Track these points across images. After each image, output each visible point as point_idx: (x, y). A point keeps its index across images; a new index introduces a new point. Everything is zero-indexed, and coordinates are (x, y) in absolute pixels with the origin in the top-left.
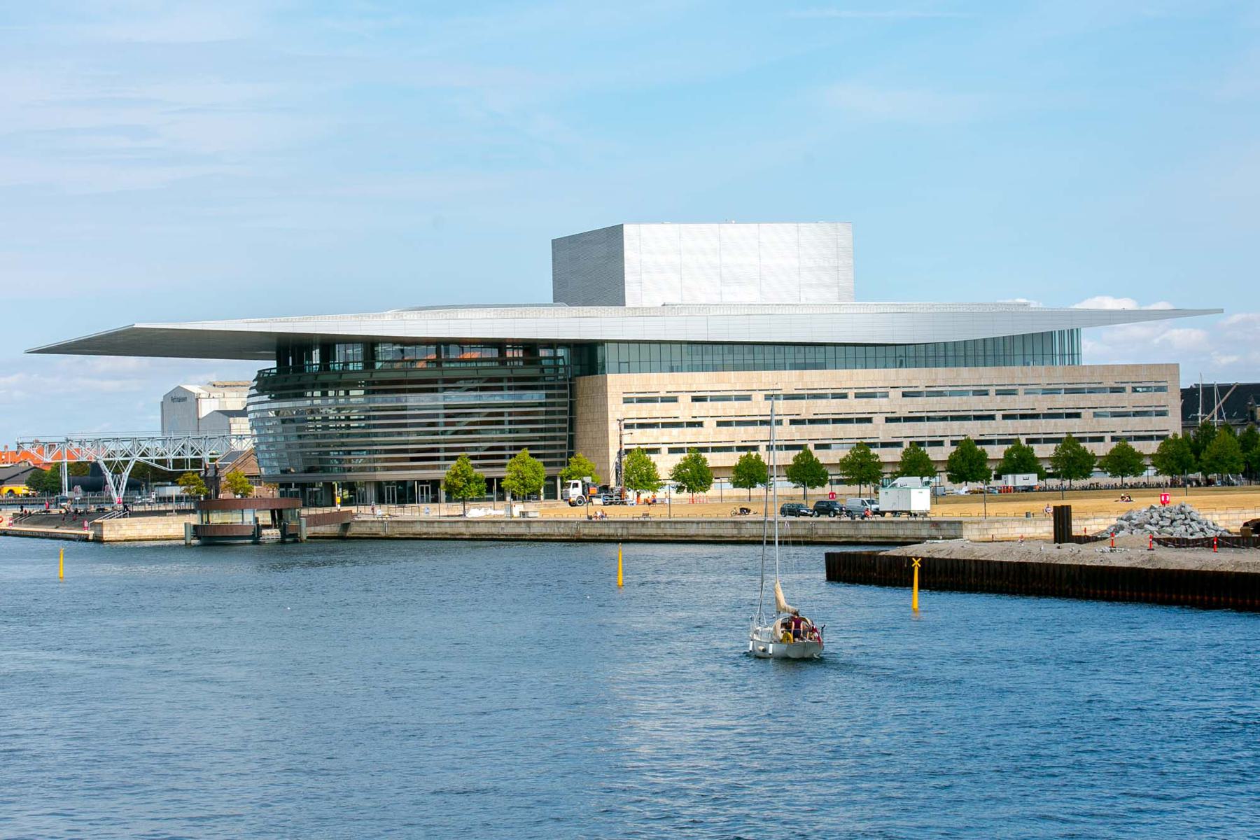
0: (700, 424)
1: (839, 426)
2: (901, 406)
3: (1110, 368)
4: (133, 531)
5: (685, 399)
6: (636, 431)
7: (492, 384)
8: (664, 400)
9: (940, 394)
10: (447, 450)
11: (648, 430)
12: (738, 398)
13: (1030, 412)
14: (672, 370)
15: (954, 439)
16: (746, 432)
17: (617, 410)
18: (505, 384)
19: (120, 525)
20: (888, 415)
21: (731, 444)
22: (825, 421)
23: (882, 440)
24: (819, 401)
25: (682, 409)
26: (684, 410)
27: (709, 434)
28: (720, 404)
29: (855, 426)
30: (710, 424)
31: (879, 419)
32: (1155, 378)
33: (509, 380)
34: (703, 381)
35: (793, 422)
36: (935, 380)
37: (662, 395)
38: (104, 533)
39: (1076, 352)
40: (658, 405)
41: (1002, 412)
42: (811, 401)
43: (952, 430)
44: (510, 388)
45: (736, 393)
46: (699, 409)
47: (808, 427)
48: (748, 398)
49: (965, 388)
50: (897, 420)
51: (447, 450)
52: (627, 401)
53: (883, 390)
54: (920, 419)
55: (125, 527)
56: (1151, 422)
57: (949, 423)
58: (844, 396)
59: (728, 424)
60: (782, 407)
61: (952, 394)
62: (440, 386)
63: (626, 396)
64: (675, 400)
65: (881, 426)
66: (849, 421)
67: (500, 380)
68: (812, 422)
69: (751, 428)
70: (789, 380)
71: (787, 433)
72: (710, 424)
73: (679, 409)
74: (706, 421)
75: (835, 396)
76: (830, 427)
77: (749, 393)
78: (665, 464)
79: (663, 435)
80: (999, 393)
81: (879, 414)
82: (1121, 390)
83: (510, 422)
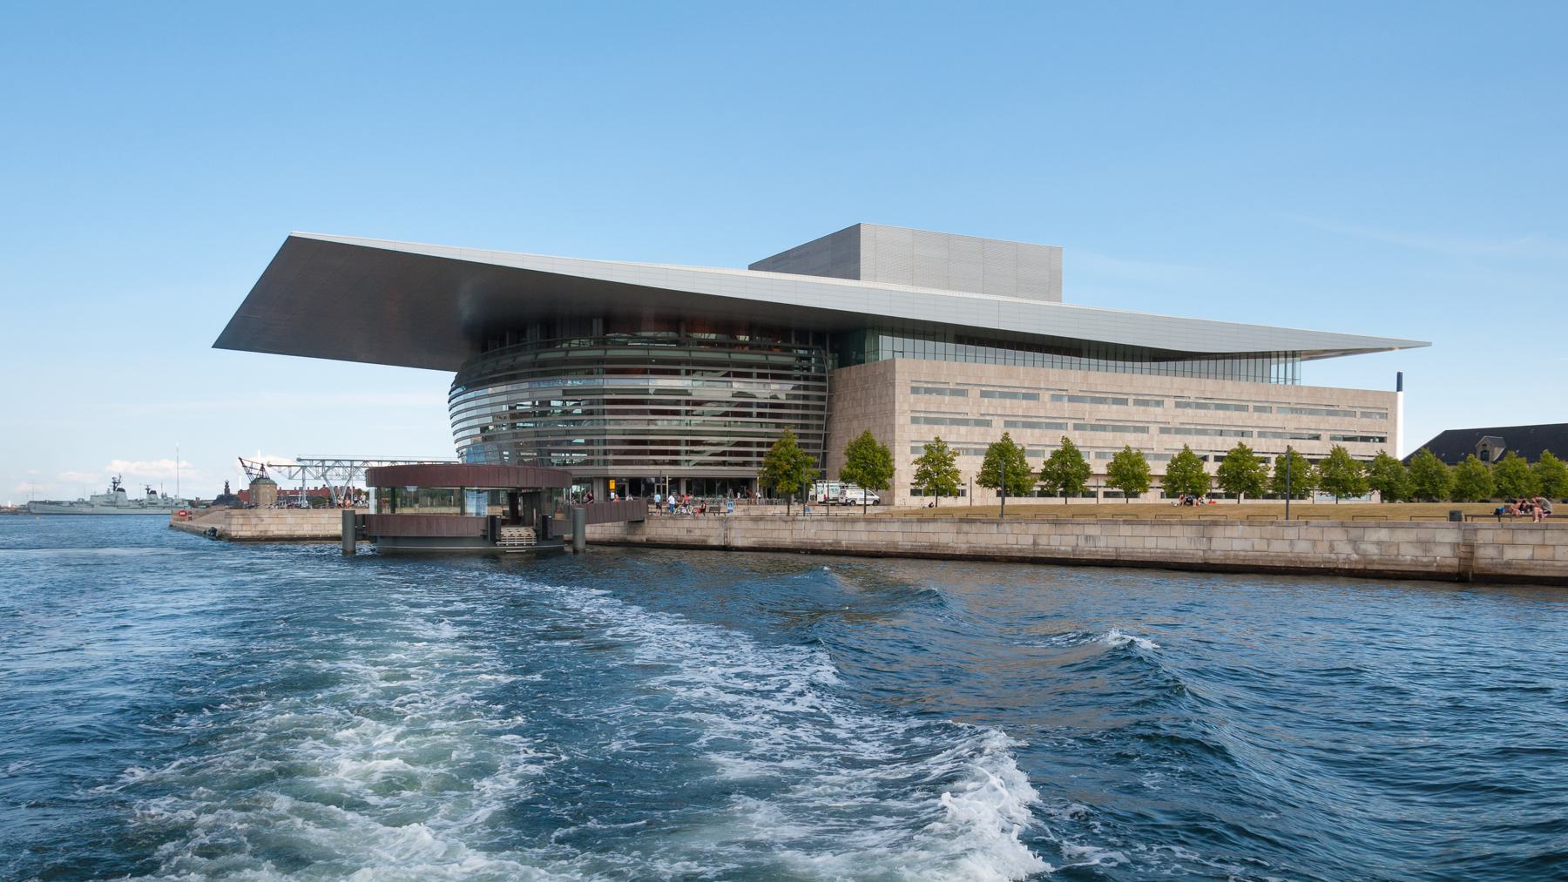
1: (1118, 434)
2: (1174, 417)
3: (1344, 392)
4: (280, 527)
5: (974, 393)
6: (925, 428)
8: (955, 392)
10: (687, 443)
11: (936, 427)
12: (1026, 397)
13: (1280, 431)
15: (1218, 454)
16: (1032, 435)
17: (904, 403)
18: (755, 371)
19: (258, 517)
20: (1162, 426)
22: (1103, 428)
23: (1155, 451)
24: (1101, 406)
26: (971, 407)
28: (1008, 402)
31: (1154, 428)
32: (1379, 404)
33: (759, 366)
36: (1203, 392)
38: (233, 528)
39: (1289, 376)
40: (947, 398)
41: (1258, 430)
42: (1093, 405)
43: (1216, 445)
44: (760, 376)
45: (1024, 391)
47: (1089, 434)
49: (1228, 402)
51: (687, 443)
52: (915, 390)
55: (268, 521)
58: (1124, 402)
60: (1067, 408)
61: (1219, 407)
62: (683, 368)
63: (914, 385)
64: (963, 393)
65: (1156, 438)
67: (750, 365)
68: (1094, 428)
69: (1037, 432)
73: (968, 404)
75: (1117, 401)
76: (1109, 435)
77: (1036, 392)
78: (969, 467)
79: (950, 433)
80: (1257, 409)
81: (1156, 425)
82: (1354, 414)
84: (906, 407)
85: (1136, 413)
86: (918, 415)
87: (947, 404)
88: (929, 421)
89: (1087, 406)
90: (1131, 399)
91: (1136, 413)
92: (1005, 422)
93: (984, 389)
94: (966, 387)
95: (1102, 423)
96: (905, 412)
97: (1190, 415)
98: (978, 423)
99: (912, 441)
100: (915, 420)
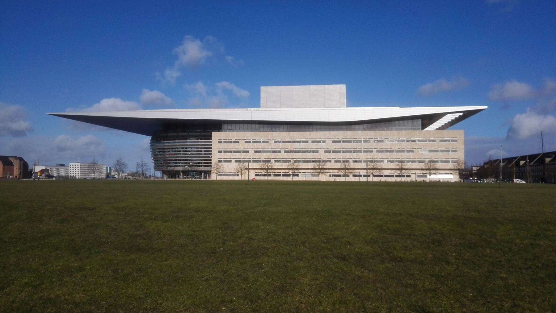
0: (248, 152)
6: (223, 154)
11: (227, 153)
12: (263, 142)
20: (325, 150)
21: (259, 160)
22: (299, 152)
25: (240, 145)
26: (241, 146)
27: (251, 155)
28: (256, 144)
29: (311, 154)
30: (252, 152)
34: (249, 135)
35: (285, 152)
37: (233, 140)
46: (247, 146)
48: (267, 142)
52: (220, 142)
53: (323, 140)
54: (340, 152)
56: (448, 155)
57: (352, 153)
58: (307, 142)
59: (259, 152)
60: (281, 145)
63: (219, 140)
64: (238, 142)
65: (322, 154)
68: (293, 152)
69: (268, 154)
71: (283, 155)
74: (250, 151)
84: (216, 148)
85: (314, 146)
86: (220, 150)
87: (231, 146)
88: (225, 152)
90: (310, 141)
91: (314, 146)
92: (255, 151)
93: (246, 140)
94: (238, 140)
95: (296, 150)
96: (216, 149)
97: (338, 146)
98: (244, 152)
99: (218, 158)
100: (220, 152)
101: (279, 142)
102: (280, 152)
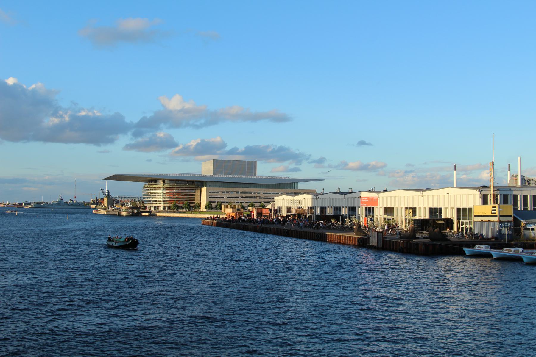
0: (224, 197)
7: (186, 189)
9: (270, 194)
14: (220, 187)
22: (248, 198)
26: (221, 195)
28: (228, 194)
30: (225, 198)
33: (189, 188)
34: (225, 189)
35: (241, 198)
44: (189, 189)
50: (261, 198)
52: (210, 192)
54: (266, 198)
58: (252, 193)
59: (229, 198)
60: (239, 195)
66: (252, 198)
67: (187, 188)
68: (245, 198)
69: (233, 199)
70: (241, 190)
72: (225, 198)
74: (225, 197)
76: (249, 199)
83: (189, 196)
88: (212, 197)
89: (244, 194)
98: (222, 197)
100: (210, 197)
101: (238, 193)
102: (239, 198)
